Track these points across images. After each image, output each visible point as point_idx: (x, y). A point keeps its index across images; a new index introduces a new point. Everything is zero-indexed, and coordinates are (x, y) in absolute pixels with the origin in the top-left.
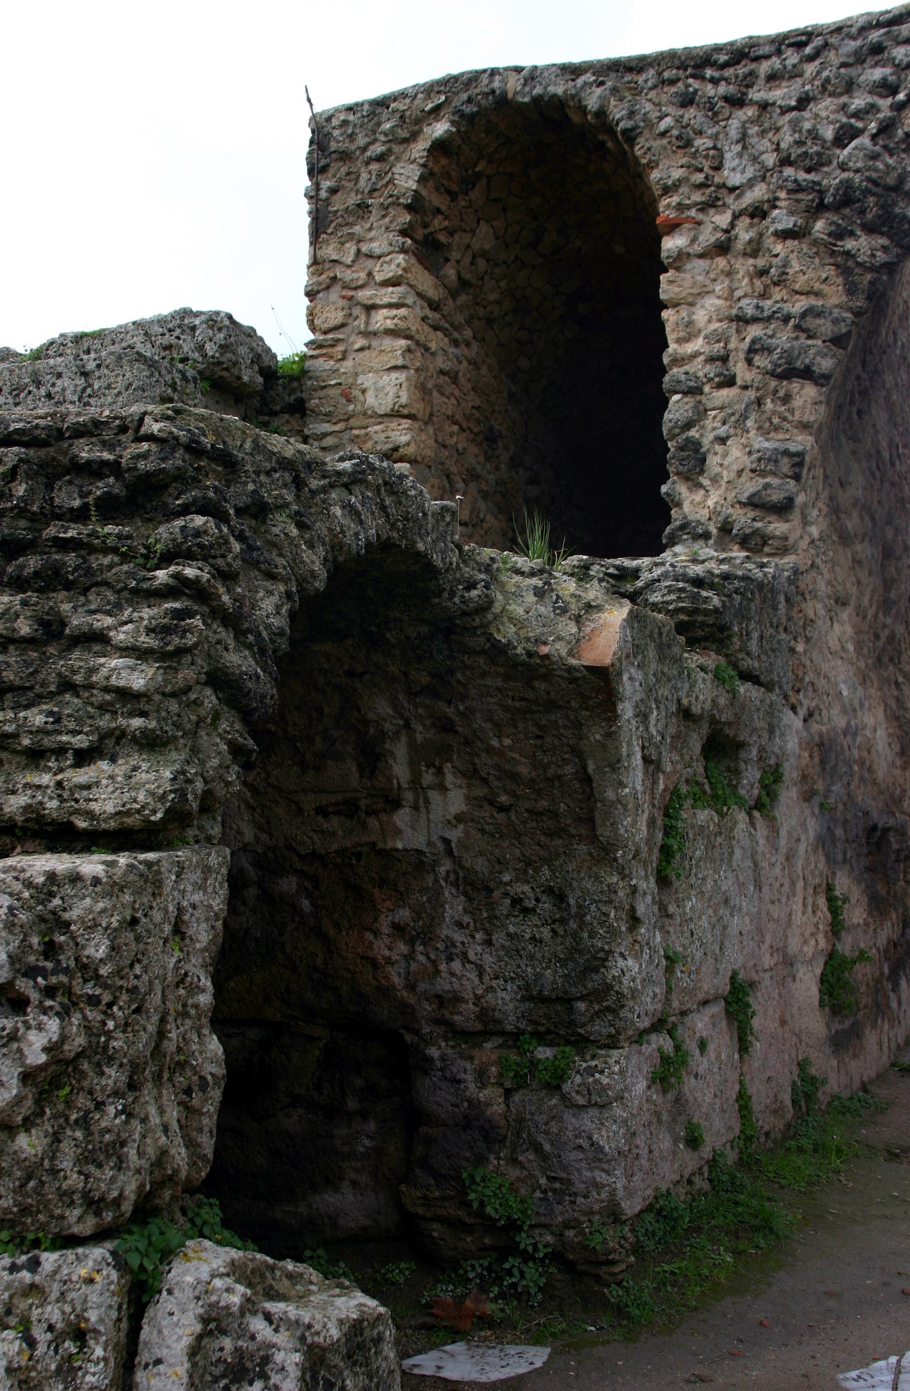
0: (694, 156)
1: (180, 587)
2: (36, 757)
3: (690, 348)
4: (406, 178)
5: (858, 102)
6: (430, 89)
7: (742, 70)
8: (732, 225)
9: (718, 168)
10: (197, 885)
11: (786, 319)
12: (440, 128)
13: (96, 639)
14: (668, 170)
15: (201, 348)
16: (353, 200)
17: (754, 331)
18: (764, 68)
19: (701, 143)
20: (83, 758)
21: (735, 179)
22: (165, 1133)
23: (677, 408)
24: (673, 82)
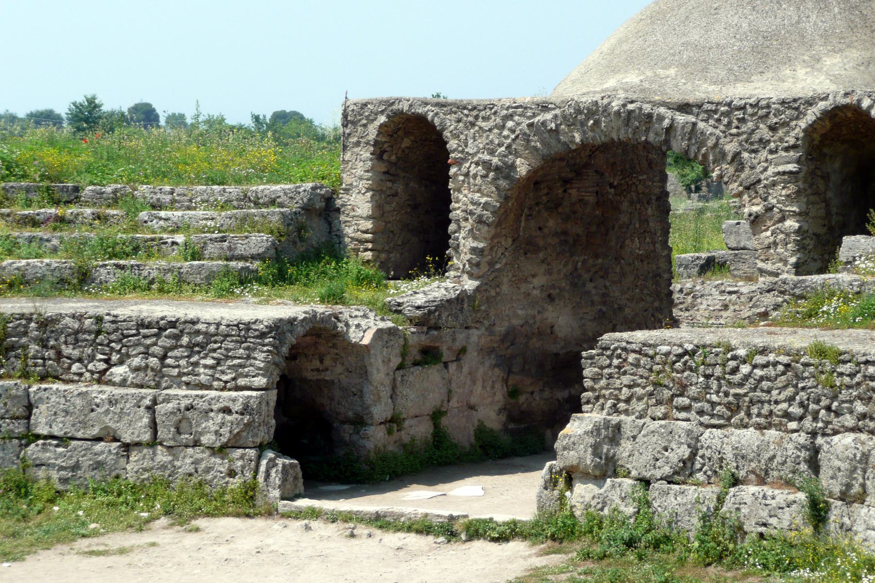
0: (460, 141)
1: (268, 351)
2: (246, 376)
3: (457, 205)
4: (372, 132)
5: (506, 133)
6: (381, 102)
7: (475, 113)
8: (470, 166)
9: (466, 146)
10: (273, 395)
11: (480, 204)
12: (382, 119)
13: (255, 359)
14: (452, 144)
15: (302, 199)
16: (355, 139)
18: (483, 113)
19: (462, 137)
20: (253, 377)
21: (471, 151)
22: (265, 434)
23: (452, 227)
24: (455, 113)
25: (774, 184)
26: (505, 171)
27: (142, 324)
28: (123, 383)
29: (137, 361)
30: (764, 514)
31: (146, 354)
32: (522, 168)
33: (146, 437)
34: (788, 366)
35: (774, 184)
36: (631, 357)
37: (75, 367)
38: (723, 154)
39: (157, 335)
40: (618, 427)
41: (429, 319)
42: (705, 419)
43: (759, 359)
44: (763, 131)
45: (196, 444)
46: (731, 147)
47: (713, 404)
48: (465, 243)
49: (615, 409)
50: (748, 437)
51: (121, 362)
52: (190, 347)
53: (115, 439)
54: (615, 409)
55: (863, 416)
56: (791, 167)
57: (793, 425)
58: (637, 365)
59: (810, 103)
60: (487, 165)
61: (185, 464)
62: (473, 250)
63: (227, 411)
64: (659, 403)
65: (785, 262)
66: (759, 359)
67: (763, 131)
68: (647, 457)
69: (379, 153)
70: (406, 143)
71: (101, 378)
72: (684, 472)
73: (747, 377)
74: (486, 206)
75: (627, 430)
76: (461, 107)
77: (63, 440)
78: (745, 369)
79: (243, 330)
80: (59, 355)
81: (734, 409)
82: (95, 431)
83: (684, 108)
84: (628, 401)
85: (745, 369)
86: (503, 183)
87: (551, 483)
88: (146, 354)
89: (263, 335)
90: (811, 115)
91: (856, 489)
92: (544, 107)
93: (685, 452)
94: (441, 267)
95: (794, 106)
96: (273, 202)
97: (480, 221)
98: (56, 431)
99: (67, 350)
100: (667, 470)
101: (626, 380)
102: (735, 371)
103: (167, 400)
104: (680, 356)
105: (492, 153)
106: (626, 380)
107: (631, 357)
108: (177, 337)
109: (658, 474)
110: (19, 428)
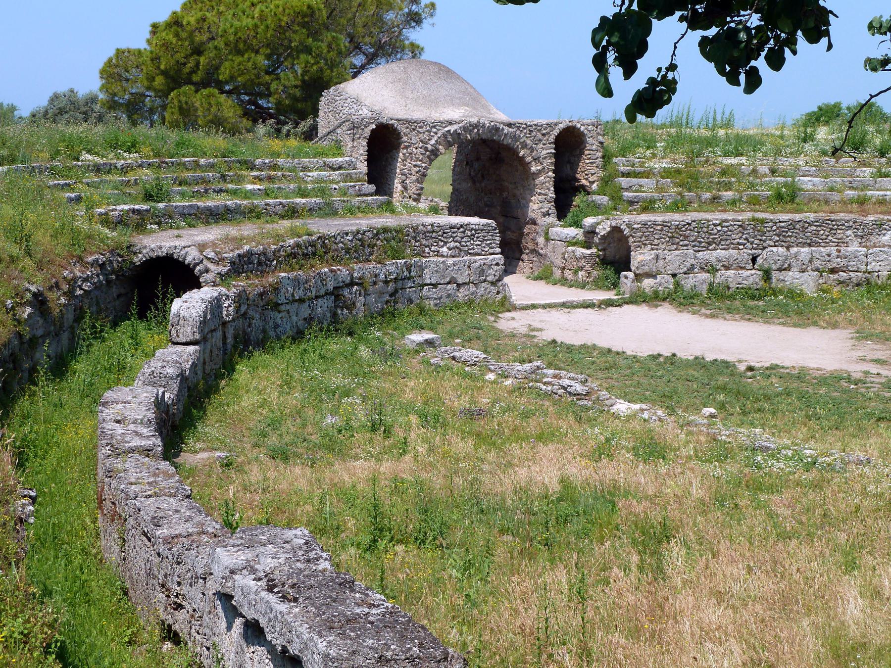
17: (417, 169)
25: (545, 158)
29: (452, 244)
30: (740, 280)
35: (545, 158)
36: (659, 228)
37: (427, 250)
42: (696, 248)
44: (539, 136)
45: (485, 281)
47: (700, 242)
50: (720, 253)
55: (777, 241)
56: (553, 151)
57: (741, 247)
58: (662, 230)
59: (556, 125)
61: (481, 291)
64: (673, 244)
65: (549, 190)
67: (539, 136)
68: (676, 265)
75: (661, 256)
76: (408, 121)
77: (435, 286)
78: (719, 228)
81: (709, 244)
83: (510, 125)
85: (719, 228)
90: (556, 132)
91: (786, 266)
92: (450, 123)
96: (340, 168)
98: (433, 282)
100: (685, 269)
103: (475, 261)
106: (657, 236)
107: (659, 228)
108: (464, 232)
109: (681, 271)
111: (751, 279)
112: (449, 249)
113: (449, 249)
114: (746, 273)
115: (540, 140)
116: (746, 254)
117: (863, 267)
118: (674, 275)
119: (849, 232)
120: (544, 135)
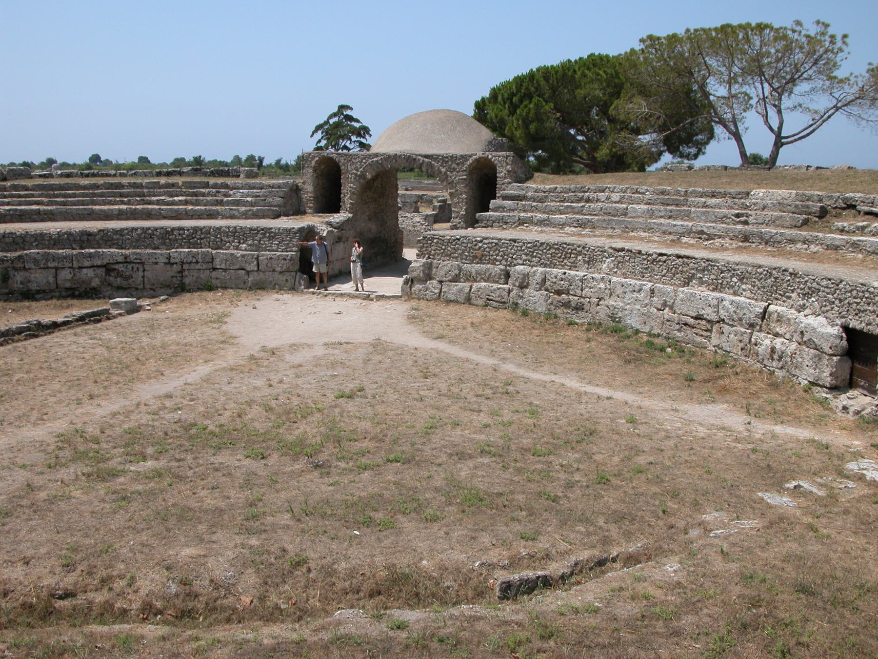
4: (313, 163)
14: (342, 168)
22: (297, 267)
23: (342, 195)
26: (363, 176)
27: (251, 229)
28: (246, 250)
29: (250, 242)
31: (254, 240)
32: (369, 176)
33: (256, 269)
34: (496, 244)
38: (441, 172)
39: (257, 233)
40: (431, 264)
41: (341, 227)
43: (486, 241)
46: (443, 170)
48: (347, 199)
49: (429, 258)
51: (244, 243)
52: (269, 237)
53: (243, 269)
54: (429, 258)
59: (470, 156)
60: (356, 174)
62: (351, 203)
63: (285, 259)
66: (486, 241)
67: (454, 165)
69: (315, 170)
70: (323, 167)
71: (237, 248)
72: (456, 279)
73: (480, 247)
74: (355, 189)
77: (225, 270)
78: (480, 245)
79: (288, 231)
80: (222, 240)
82: (237, 267)
83: (427, 156)
84: (434, 255)
86: (362, 181)
87: (406, 282)
88: (254, 240)
89: (295, 233)
90: (470, 161)
93: (457, 272)
94: (337, 210)
95: (464, 158)
96: (279, 187)
97: (353, 193)
99: (225, 239)
101: (433, 248)
102: (476, 245)
104: (454, 240)
105: (357, 170)
110: (210, 266)
111: (498, 293)
112: (249, 245)
113: (249, 245)
114: (495, 286)
115: (454, 169)
116: (498, 268)
117: (579, 292)
118: (441, 282)
119: (580, 258)
120: (458, 164)
